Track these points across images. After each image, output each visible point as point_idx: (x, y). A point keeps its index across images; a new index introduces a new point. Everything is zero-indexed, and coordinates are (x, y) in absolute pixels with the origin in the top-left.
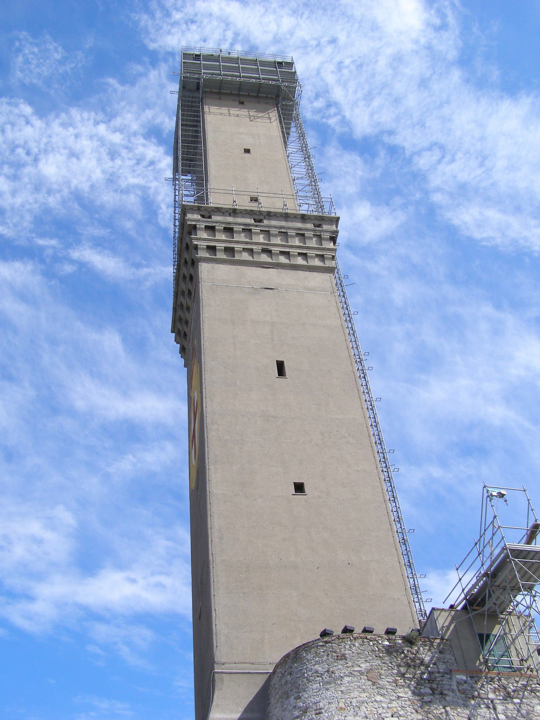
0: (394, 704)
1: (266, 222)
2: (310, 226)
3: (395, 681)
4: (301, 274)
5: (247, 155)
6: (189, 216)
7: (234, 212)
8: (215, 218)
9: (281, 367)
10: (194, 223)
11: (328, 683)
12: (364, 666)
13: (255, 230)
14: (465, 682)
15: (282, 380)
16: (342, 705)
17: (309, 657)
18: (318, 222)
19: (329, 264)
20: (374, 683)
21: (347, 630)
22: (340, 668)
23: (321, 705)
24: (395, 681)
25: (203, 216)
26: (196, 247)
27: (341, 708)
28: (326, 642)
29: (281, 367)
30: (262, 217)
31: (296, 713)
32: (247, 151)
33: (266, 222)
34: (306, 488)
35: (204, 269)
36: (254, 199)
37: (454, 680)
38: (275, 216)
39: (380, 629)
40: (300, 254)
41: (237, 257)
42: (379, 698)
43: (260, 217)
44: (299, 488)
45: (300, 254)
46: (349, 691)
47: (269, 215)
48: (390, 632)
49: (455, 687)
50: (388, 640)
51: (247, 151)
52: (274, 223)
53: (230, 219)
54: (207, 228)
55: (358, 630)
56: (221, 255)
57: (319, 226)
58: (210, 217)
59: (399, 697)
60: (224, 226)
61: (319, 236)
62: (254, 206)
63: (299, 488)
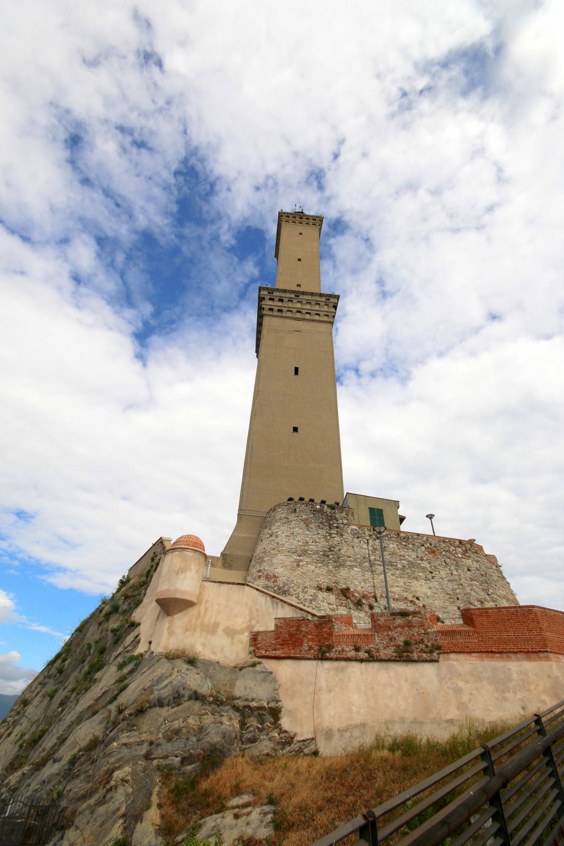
0: (315, 536)
1: (301, 297)
2: (324, 299)
3: (319, 526)
4: (315, 324)
5: (299, 262)
6: (262, 292)
7: (285, 291)
8: (276, 294)
9: (296, 371)
11: (285, 523)
12: (304, 517)
13: (295, 301)
14: (356, 530)
15: (296, 376)
16: (288, 534)
17: (279, 510)
18: (327, 298)
19: (331, 319)
20: (307, 526)
21: (301, 499)
22: (292, 517)
23: (279, 533)
24: (319, 526)
25: (269, 293)
26: (263, 309)
27: (288, 536)
28: (288, 504)
29: (296, 371)
30: (299, 294)
31: (268, 536)
32: (299, 260)
33: (301, 297)
34: (299, 430)
36: (299, 285)
37: (350, 528)
39: (317, 501)
40: (316, 314)
41: (284, 314)
42: (308, 533)
43: (298, 294)
44: (295, 429)
45: (316, 314)
46: (294, 528)
47: (303, 293)
48: (323, 502)
49: (349, 531)
51: (299, 260)
52: (305, 297)
53: (283, 295)
55: (307, 499)
56: (275, 313)
57: (329, 300)
58: (272, 293)
59: (318, 534)
62: (298, 289)
63: (295, 429)
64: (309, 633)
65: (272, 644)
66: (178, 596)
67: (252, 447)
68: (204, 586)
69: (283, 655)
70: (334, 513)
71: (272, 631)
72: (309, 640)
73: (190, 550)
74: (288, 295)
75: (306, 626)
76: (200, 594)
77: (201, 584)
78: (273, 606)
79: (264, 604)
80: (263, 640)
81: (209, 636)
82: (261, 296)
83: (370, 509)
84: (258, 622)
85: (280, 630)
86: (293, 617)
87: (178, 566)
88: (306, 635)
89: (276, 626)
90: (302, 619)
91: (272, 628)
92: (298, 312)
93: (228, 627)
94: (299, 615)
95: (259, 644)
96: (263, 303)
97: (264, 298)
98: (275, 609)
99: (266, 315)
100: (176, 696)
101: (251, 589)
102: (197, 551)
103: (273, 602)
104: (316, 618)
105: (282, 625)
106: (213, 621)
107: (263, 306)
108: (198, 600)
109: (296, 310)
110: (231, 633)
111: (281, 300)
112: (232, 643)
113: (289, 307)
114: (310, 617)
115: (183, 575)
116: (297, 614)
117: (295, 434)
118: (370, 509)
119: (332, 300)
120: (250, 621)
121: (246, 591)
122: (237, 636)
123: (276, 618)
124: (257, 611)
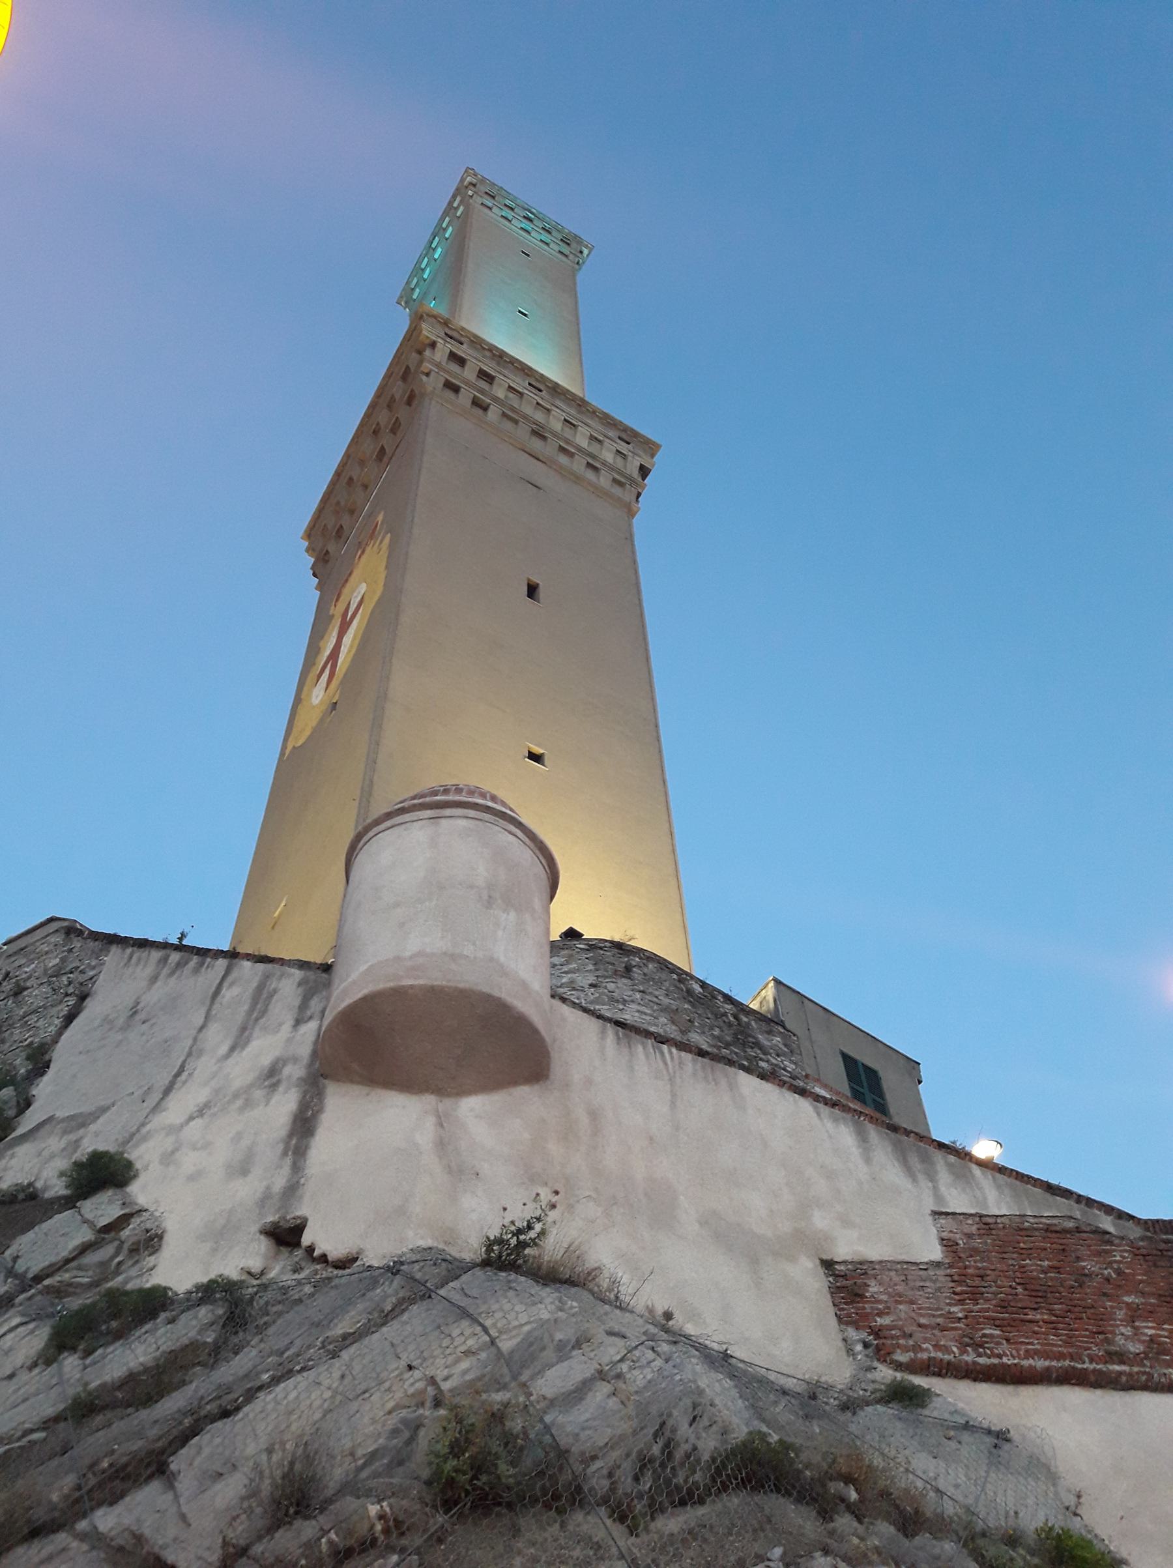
64: (1123, 1282)
65: (949, 1316)
69: (1041, 1364)
71: (937, 1265)
72: (1134, 1315)
75: (1099, 1254)
80: (899, 1298)
83: (846, 1058)
84: (846, 1222)
85: (973, 1264)
88: (1108, 1289)
89: (948, 1244)
90: (1070, 1224)
95: (880, 1314)
98: (921, 1177)
105: (977, 1243)
114: (1107, 1224)
118: (846, 1058)
121: (746, 1091)
123: (936, 1214)
124: (830, 1175)
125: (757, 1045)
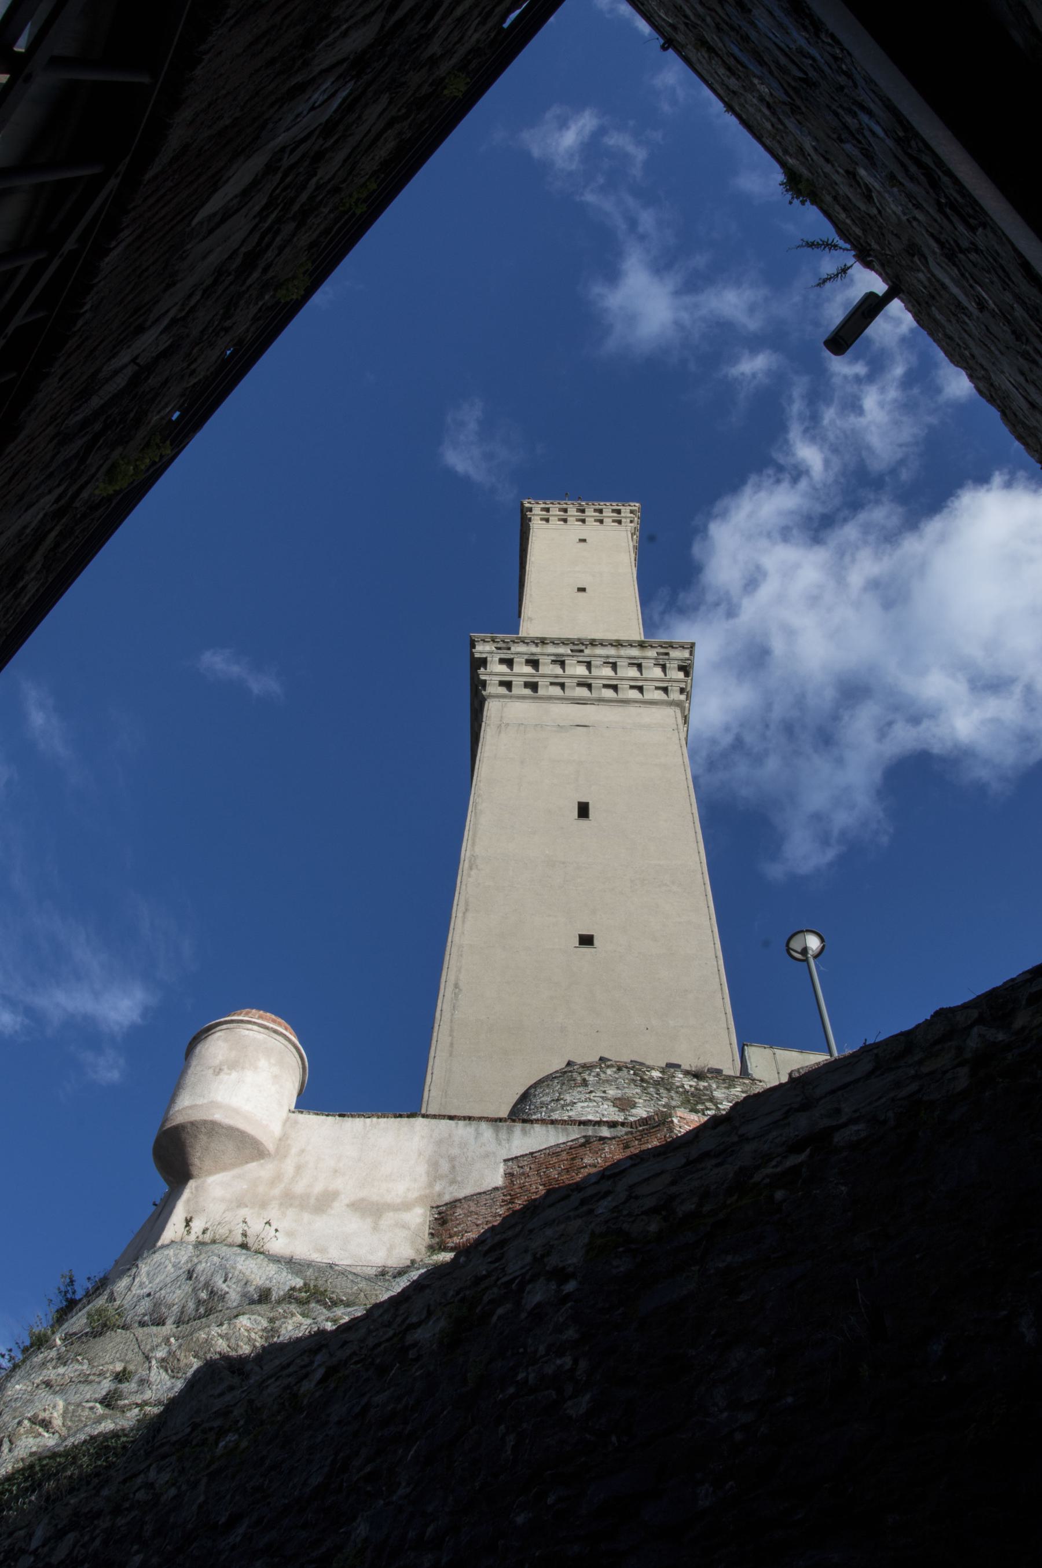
1: (587, 651)
2: (652, 653)
4: (632, 710)
9: (583, 810)
10: (484, 656)
15: (583, 822)
25: (497, 648)
28: (565, 1072)
29: (583, 810)
30: (583, 647)
32: (582, 590)
33: (587, 651)
34: (595, 941)
35: (492, 709)
38: (602, 645)
50: (663, 1072)
51: (582, 590)
52: (599, 651)
54: (502, 661)
58: (509, 649)
60: (526, 657)
61: (664, 667)
66: (218, 1116)
67: (456, 986)
68: (296, 1122)
70: (708, 1088)
71: (496, 1189)
73: (255, 1027)
74: (551, 649)
76: (284, 1138)
77: (287, 1119)
78: (497, 1138)
79: (472, 1141)
81: (306, 1216)
82: (477, 655)
86: (558, 1145)
87: (220, 1058)
89: (509, 1175)
90: (582, 1140)
91: (497, 1178)
92: (580, 685)
93: (363, 1200)
94: (575, 1134)
96: (482, 669)
97: (484, 662)
99: (491, 696)
100: (204, 1295)
101: (434, 1121)
102: (275, 1032)
103: (497, 1131)
104: (621, 1131)
106: (318, 1188)
107: (483, 677)
108: (277, 1150)
109: (576, 681)
110: (371, 1210)
111: (534, 663)
112: (375, 1228)
113: (557, 677)
114: (605, 1132)
115: (234, 1075)
116: (567, 1135)
117: (586, 950)
119: (675, 654)
120: (431, 1185)
122: (391, 1214)
123: (505, 1161)
125: (712, 1099)
